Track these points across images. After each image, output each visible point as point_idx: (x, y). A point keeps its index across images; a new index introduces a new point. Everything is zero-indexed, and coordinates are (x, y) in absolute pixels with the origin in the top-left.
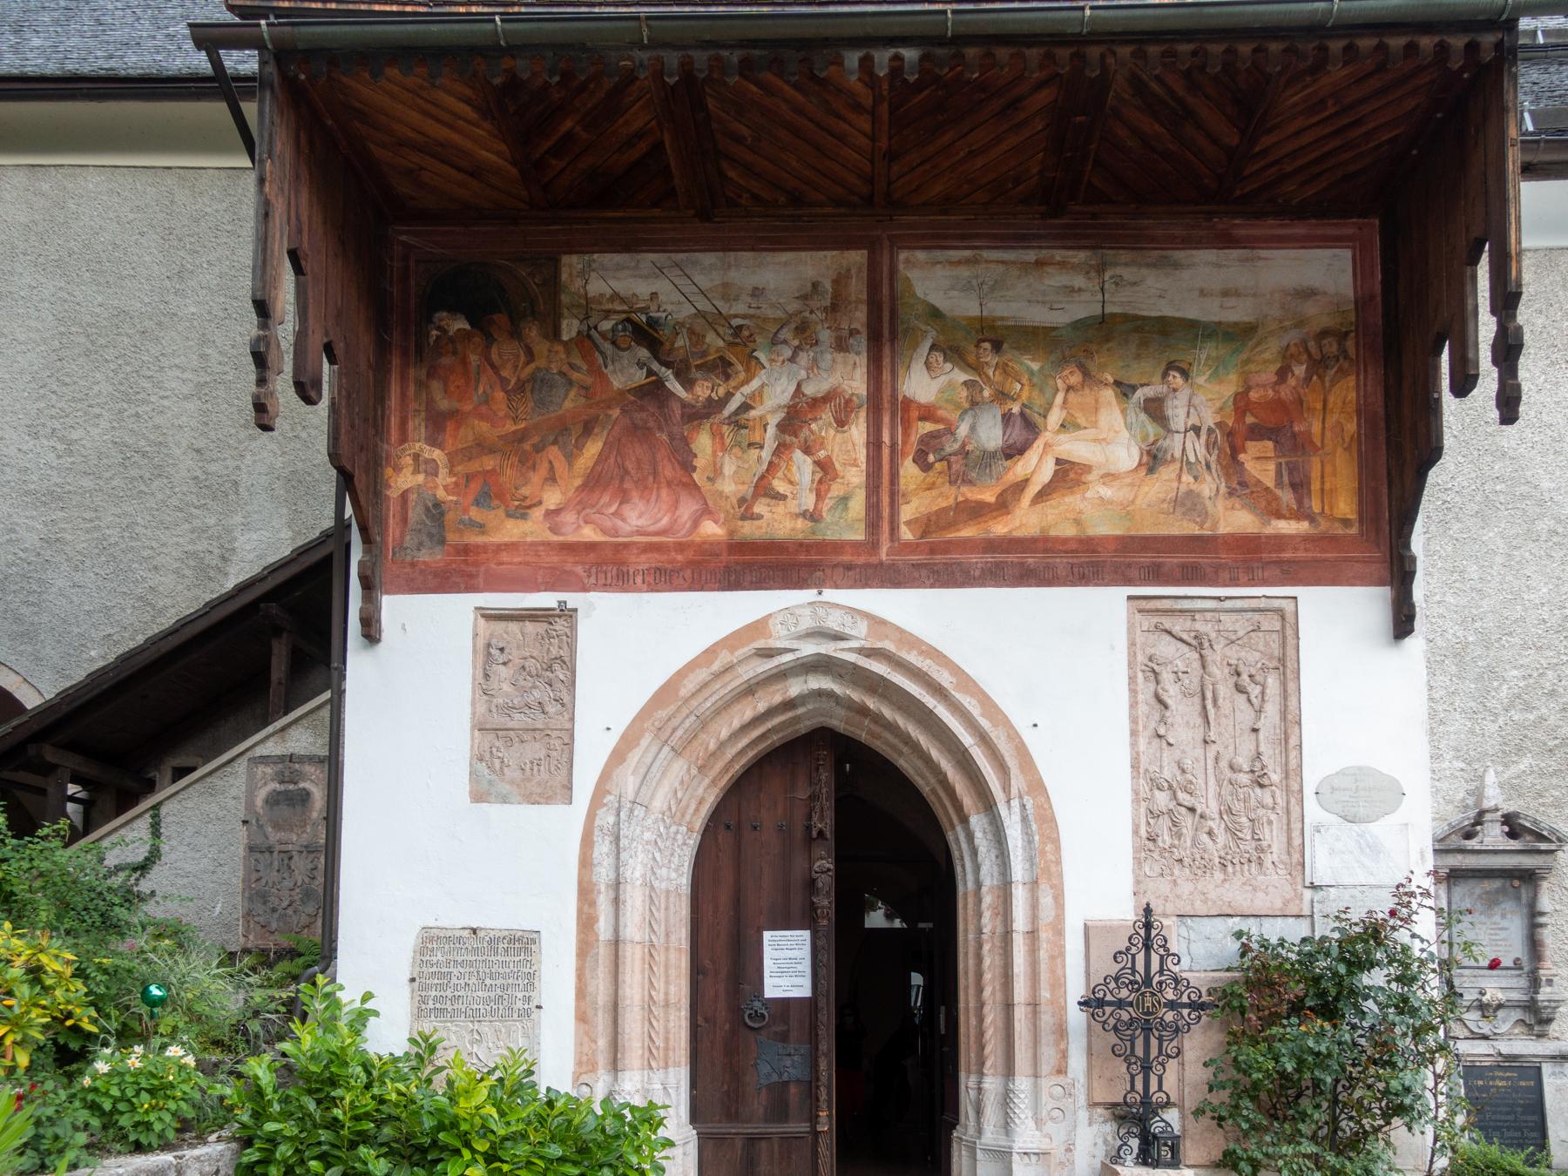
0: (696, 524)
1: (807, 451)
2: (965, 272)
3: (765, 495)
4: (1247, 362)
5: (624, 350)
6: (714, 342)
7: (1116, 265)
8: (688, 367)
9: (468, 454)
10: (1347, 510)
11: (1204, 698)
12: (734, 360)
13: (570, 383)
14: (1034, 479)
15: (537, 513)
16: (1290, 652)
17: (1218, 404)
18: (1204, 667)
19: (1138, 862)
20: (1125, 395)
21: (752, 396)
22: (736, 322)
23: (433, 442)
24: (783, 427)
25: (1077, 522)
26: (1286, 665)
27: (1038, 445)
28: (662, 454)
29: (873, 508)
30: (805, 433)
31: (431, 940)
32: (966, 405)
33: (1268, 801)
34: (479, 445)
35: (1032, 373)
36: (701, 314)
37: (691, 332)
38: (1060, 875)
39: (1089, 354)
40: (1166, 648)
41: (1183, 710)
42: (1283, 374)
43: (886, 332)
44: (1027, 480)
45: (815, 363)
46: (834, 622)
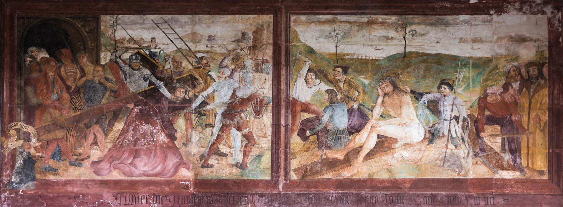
0: (176, 170)
1: (239, 129)
2: (327, 28)
3: (215, 154)
4: (485, 80)
5: (136, 70)
6: (187, 66)
7: (413, 24)
8: (172, 81)
9: (48, 129)
10: (542, 165)
13: (106, 89)
14: (365, 146)
15: (87, 163)
17: (469, 104)
20: (417, 99)
21: (208, 97)
22: (199, 55)
23: (29, 121)
24: (225, 115)
25: (389, 171)
27: (368, 127)
29: (275, 161)
30: (237, 118)
32: (327, 104)
34: (54, 124)
35: (365, 86)
36: (179, 50)
37: (174, 60)
39: (397, 75)
42: (506, 87)
44: (361, 147)
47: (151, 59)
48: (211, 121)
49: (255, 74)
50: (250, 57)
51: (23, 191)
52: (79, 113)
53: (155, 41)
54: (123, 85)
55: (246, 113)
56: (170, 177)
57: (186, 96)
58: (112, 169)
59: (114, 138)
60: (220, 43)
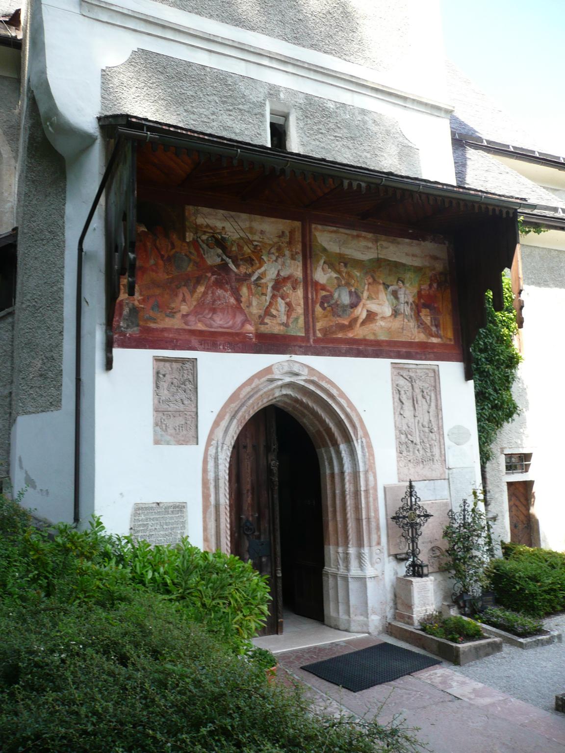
1: (283, 298)
2: (334, 235)
3: (269, 315)
6: (247, 250)
11: (413, 400)
12: (255, 258)
13: (190, 260)
15: (178, 316)
16: (438, 384)
18: (413, 389)
19: (398, 461)
22: (255, 243)
24: (274, 288)
26: (436, 388)
27: (361, 304)
29: (306, 323)
30: (281, 291)
31: (139, 509)
33: (434, 438)
35: (357, 277)
36: (241, 238)
37: (238, 245)
38: (375, 468)
39: (374, 272)
40: (402, 382)
41: (408, 404)
42: (430, 286)
43: (308, 254)
45: (283, 264)
46: (296, 369)
51: (130, 335)
54: (202, 258)
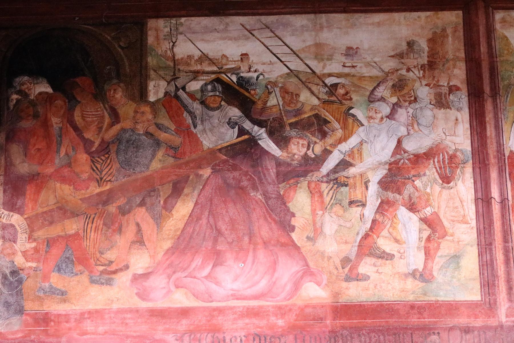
0: (297, 286)
1: (412, 208)
6: (308, 100)
8: (282, 126)
9: (49, 218)
12: (330, 118)
13: (158, 143)
15: (123, 279)
22: (330, 81)
24: (385, 184)
28: (257, 214)
30: (408, 190)
34: (60, 208)
36: (293, 73)
37: (284, 91)
43: (487, 89)
45: (414, 121)
47: (242, 90)
48: (358, 195)
49: (436, 111)
50: (424, 82)
52: (108, 187)
53: (248, 58)
55: (424, 179)
56: (285, 299)
57: (310, 153)
58: (173, 288)
59: (176, 231)
60: (369, 59)
